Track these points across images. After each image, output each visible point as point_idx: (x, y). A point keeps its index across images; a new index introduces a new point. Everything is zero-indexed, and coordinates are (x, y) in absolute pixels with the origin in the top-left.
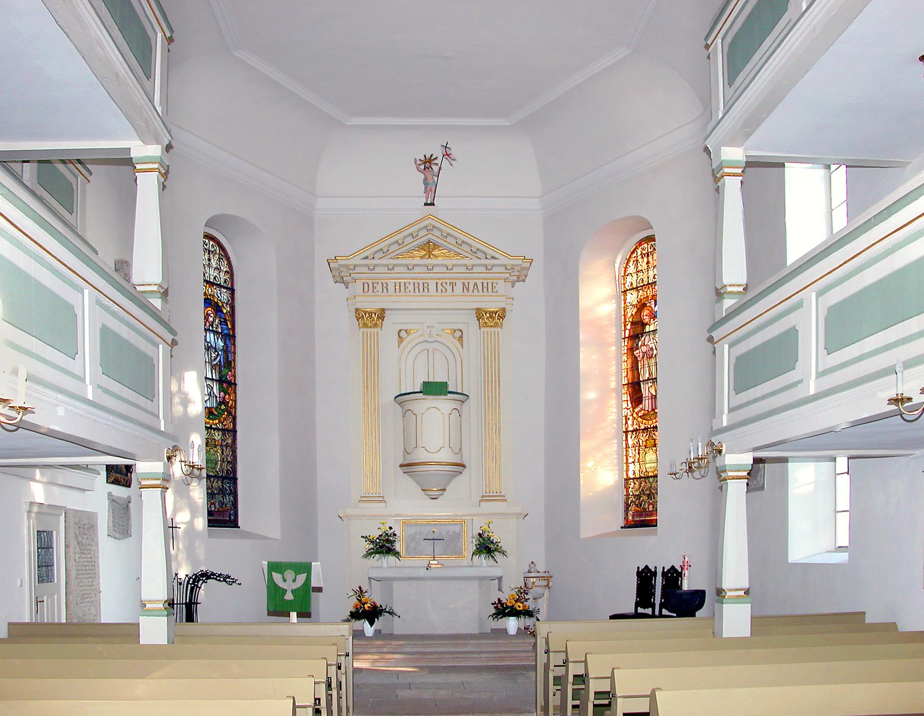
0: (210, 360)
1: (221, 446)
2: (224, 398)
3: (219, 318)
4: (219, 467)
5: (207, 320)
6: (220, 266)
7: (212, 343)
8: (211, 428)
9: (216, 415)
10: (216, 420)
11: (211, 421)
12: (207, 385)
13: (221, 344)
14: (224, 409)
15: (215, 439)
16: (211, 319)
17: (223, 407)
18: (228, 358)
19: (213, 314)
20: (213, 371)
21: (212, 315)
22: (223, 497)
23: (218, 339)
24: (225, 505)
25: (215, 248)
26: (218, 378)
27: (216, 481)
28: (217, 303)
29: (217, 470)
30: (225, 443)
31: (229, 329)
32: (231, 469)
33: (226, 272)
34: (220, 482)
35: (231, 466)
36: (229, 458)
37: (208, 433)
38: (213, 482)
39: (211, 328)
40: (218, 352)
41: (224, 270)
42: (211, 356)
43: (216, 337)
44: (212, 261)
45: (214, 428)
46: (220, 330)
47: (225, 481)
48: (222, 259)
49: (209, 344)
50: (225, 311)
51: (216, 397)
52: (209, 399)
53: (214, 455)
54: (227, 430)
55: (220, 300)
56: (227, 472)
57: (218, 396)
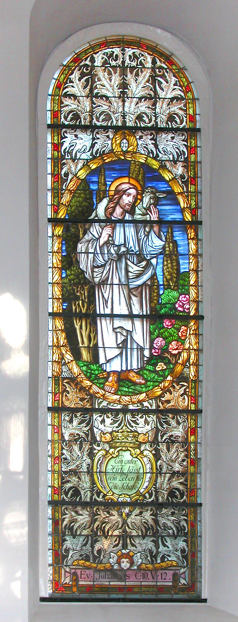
0: (123, 280)
1: (155, 442)
2: (165, 350)
3: (152, 192)
4: (146, 484)
5: (118, 203)
6: (155, 92)
8: (125, 410)
9: (140, 384)
10: (141, 393)
12: (114, 329)
15: (137, 432)
16: (127, 200)
17: (160, 366)
18: (178, 269)
19: (135, 187)
22: (156, 542)
24: (163, 559)
28: (146, 167)
32: (181, 487)
33: (172, 99)
35: (181, 481)
36: (177, 465)
38: (128, 515)
40: (148, 261)
41: (169, 96)
42: (127, 271)
45: (132, 412)
47: (164, 511)
48: (163, 76)
50: (167, 176)
51: (142, 349)
52: (121, 354)
53: (131, 462)
54: (175, 412)
55: (156, 158)
56: (171, 493)
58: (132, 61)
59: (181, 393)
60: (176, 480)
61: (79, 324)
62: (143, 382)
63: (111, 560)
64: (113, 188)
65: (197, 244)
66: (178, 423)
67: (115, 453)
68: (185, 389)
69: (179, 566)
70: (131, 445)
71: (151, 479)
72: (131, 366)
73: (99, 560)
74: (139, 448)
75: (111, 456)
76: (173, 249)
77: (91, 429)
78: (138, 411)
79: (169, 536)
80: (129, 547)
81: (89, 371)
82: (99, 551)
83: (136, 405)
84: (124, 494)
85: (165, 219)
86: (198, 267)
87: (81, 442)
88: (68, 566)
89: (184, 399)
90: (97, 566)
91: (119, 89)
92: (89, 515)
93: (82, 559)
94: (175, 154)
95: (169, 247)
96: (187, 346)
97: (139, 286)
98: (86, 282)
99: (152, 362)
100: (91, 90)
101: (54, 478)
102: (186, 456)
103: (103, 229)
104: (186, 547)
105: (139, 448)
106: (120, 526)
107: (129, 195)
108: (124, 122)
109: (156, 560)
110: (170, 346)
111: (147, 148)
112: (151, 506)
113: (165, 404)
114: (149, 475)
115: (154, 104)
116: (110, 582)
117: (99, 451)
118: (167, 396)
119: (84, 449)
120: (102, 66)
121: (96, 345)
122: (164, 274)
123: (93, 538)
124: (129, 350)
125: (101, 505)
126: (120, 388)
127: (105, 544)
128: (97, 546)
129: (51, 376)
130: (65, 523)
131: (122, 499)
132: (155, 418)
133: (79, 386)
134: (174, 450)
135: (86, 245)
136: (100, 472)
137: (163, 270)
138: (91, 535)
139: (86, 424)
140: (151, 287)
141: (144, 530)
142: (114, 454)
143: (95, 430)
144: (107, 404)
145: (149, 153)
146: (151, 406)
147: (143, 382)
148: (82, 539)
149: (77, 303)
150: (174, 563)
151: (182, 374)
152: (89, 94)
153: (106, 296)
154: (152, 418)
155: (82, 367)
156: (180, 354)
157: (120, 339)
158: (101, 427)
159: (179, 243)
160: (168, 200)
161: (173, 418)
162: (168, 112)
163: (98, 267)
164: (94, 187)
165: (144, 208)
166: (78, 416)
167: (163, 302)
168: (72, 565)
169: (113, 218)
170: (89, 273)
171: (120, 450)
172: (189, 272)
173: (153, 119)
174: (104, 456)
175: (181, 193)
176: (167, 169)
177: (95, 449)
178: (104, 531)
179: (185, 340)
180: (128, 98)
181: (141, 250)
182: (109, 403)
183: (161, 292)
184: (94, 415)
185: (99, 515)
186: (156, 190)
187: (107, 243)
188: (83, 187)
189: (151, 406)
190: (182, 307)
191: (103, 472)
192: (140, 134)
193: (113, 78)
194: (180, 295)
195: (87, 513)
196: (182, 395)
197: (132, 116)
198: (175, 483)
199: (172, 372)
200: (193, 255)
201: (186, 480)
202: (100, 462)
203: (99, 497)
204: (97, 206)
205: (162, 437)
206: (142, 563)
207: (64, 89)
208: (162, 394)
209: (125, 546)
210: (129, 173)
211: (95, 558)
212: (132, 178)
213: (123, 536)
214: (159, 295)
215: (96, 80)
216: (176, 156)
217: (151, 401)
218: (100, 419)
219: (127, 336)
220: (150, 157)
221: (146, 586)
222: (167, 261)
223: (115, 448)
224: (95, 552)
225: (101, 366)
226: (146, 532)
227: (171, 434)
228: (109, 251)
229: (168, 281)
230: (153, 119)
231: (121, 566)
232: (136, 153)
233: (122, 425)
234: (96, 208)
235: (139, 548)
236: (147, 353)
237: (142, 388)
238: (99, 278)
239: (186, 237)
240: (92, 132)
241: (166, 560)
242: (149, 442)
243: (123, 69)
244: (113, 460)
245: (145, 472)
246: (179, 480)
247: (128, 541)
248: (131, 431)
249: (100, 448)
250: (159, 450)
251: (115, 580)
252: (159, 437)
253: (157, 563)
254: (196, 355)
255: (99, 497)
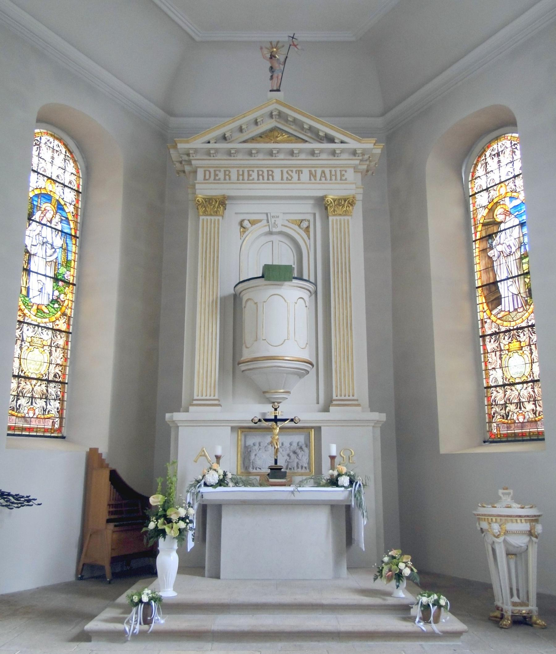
45: (42, 327)
78: (45, 327)
113: (56, 326)
118: (57, 322)
218: (27, 328)
233: (37, 334)
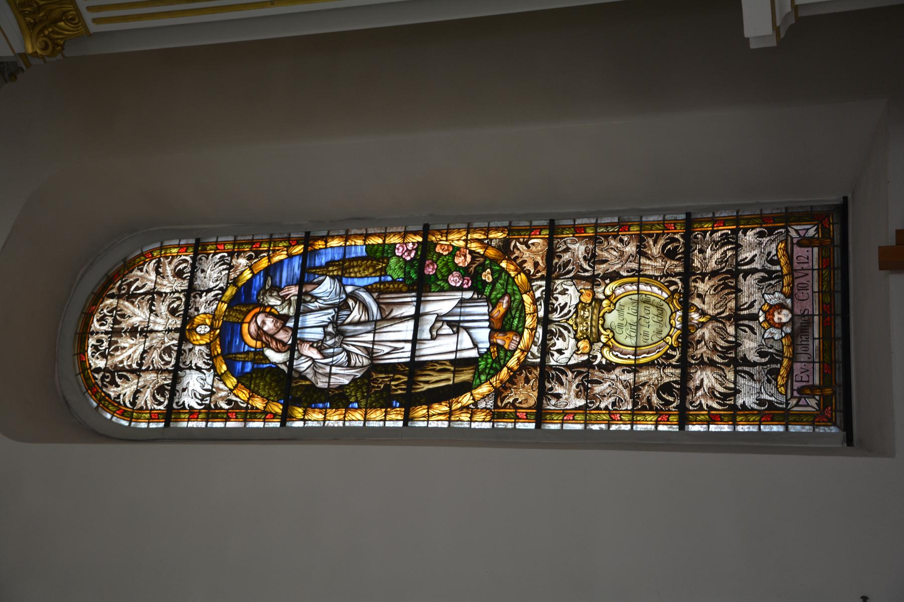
0: (369, 328)
1: (593, 280)
2: (465, 272)
3: (264, 294)
4: (655, 289)
5: (272, 337)
6: (146, 294)
7: (325, 318)
8: (545, 322)
9: (510, 302)
10: (522, 301)
11: (529, 321)
12: (433, 338)
13: (326, 288)
14: (492, 274)
15: (577, 305)
16: (269, 325)
17: (487, 277)
18: (362, 258)
19: (256, 316)
20: (397, 312)
21: (260, 319)
22: (747, 273)
23: (316, 298)
24: (773, 262)
25: (105, 311)
26: (411, 298)
27: (697, 302)
28: (232, 303)
29: (665, 295)
30: (586, 267)
31: (290, 257)
32: (662, 242)
33: (158, 273)
34: (702, 287)
35: (651, 243)
36: (628, 249)
37: (561, 335)
38: (703, 313)
39: (291, 324)
41: (153, 276)
42: (359, 323)
43: (312, 306)
44: (135, 320)
45: (547, 312)
46: (294, 290)
47: (697, 264)
48: (130, 285)
49: (330, 329)
50: (247, 275)
51: (462, 301)
52: (467, 329)
53: (620, 311)
54: (551, 254)
55: (223, 290)
56: (669, 255)
57: (459, 295)
58: (107, 322)
59: (525, 248)
60: (651, 250)
61: (422, 385)
62: (506, 298)
63: (776, 337)
64: (252, 343)
65: (333, 237)
66: (567, 250)
67: (608, 334)
68: (521, 243)
69: (786, 240)
70: (595, 311)
71: (648, 284)
72: (484, 315)
73: (777, 355)
74: (601, 301)
75: (612, 340)
76: (336, 265)
77: (571, 367)
79: (736, 255)
80: (754, 310)
81: (487, 371)
82: (762, 354)
83: (539, 307)
84: (670, 320)
85: (299, 276)
86: (361, 235)
87: (588, 382)
88: (787, 400)
89: (533, 244)
90: (787, 357)
91: (136, 338)
92: (703, 370)
93: (776, 380)
94: (221, 268)
95: (333, 271)
96: (462, 243)
97: (379, 308)
98: (367, 375)
99: (480, 287)
100: (132, 371)
101: (643, 421)
102: (615, 237)
103: (302, 355)
104: (754, 231)
105: (601, 301)
106: (720, 325)
107: (264, 322)
108: (176, 330)
109: (777, 271)
110: (461, 265)
111: (211, 302)
112: (689, 282)
113: (539, 268)
114: (642, 287)
115: (160, 294)
116: (814, 339)
117: (603, 356)
118: (529, 266)
119: (600, 378)
120: (107, 358)
121: (452, 362)
122: (366, 276)
123: (739, 363)
124: (462, 318)
125: (687, 352)
126: (514, 328)
127: (749, 346)
128: (753, 357)
129: (491, 423)
130: (715, 405)
131: (678, 323)
132: (558, 282)
133: (508, 385)
134: (606, 254)
135: (320, 376)
136: (635, 354)
137: (362, 277)
138: (735, 367)
139: (562, 374)
140: (381, 292)
141: (726, 291)
142: (608, 335)
143: (572, 362)
144: (536, 346)
145: (216, 299)
146: (541, 286)
147: (506, 298)
148: (741, 381)
149: (393, 387)
150: (782, 246)
151: (498, 248)
152: (137, 375)
153: (387, 350)
154: (559, 285)
155: (480, 380)
156: (471, 252)
157: (446, 330)
158: (567, 353)
159: (329, 258)
160: (275, 275)
161: (560, 257)
162: (171, 278)
163: (349, 360)
164: (249, 367)
165: (282, 303)
166: (550, 386)
167: (402, 276)
168: (786, 395)
169: (290, 342)
170: (357, 372)
171: (603, 326)
172: (366, 245)
173: (177, 295)
174: (612, 349)
175: (270, 258)
176: (238, 276)
177: (601, 362)
178: (728, 349)
179: (453, 247)
180: (148, 327)
181: (332, 306)
182: (534, 343)
183: (389, 279)
184: (551, 364)
185: (702, 355)
186: (261, 290)
187: (320, 350)
188: (246, 381)
189: (541, 286)
190: (409, 252)
191: (636, 350)
192: (192, 310)
193: (123, 345)
194: (394, 255)
195: (699, 372)
196: (528, 247)
197: (170, 321)
198: (656, 250)
199: (495, 261)
200: (346, 241)
201: (651, 236)
202: (619, 355)
203: (674, 356)
204: (272, 363)
205: (585, 271)
206: (781, 292)
207: (125, 406)
208: (524, 272)
209: (755, 317)
210: (238, 323)
211: (772, 361)
212: (243, 319)
213: (736, 321)
214: (394, 281)
215: (121, 365)
216: (225, 267)
217: (534, 288)
218: (556, 355)
219: (444, 321)
220: (221, 298)
221: (820, 284)
222: (350, 273)
223: (599, 334)
224: (763, 360)
225: (481, 355)
226: (731, 287)
227: (582, 260)
228: (330, 347)
229: (375, 271)
230: (177, 295)
231: (787, 323)
232: (214, 315)
233: (566, 325)
234: (275, 364)
235: (757, 296)
236: (468, 295)
237: (515, 299)
238: (364, 359)
239: (323, 250)
240: (182, 369)
241: (775, 258)
242: (592, 289)
243: (116, 332)
244: (617, 336)
245: (636, 292)
246: (649, 246)
247: (745, 312)
248: (576, 312)
249: (599, 356)
250: (604, 274)
251: (810, 331)
252: (587, 274)
253: (781, 271)
254: (474, 232)
255: (674, 356)
